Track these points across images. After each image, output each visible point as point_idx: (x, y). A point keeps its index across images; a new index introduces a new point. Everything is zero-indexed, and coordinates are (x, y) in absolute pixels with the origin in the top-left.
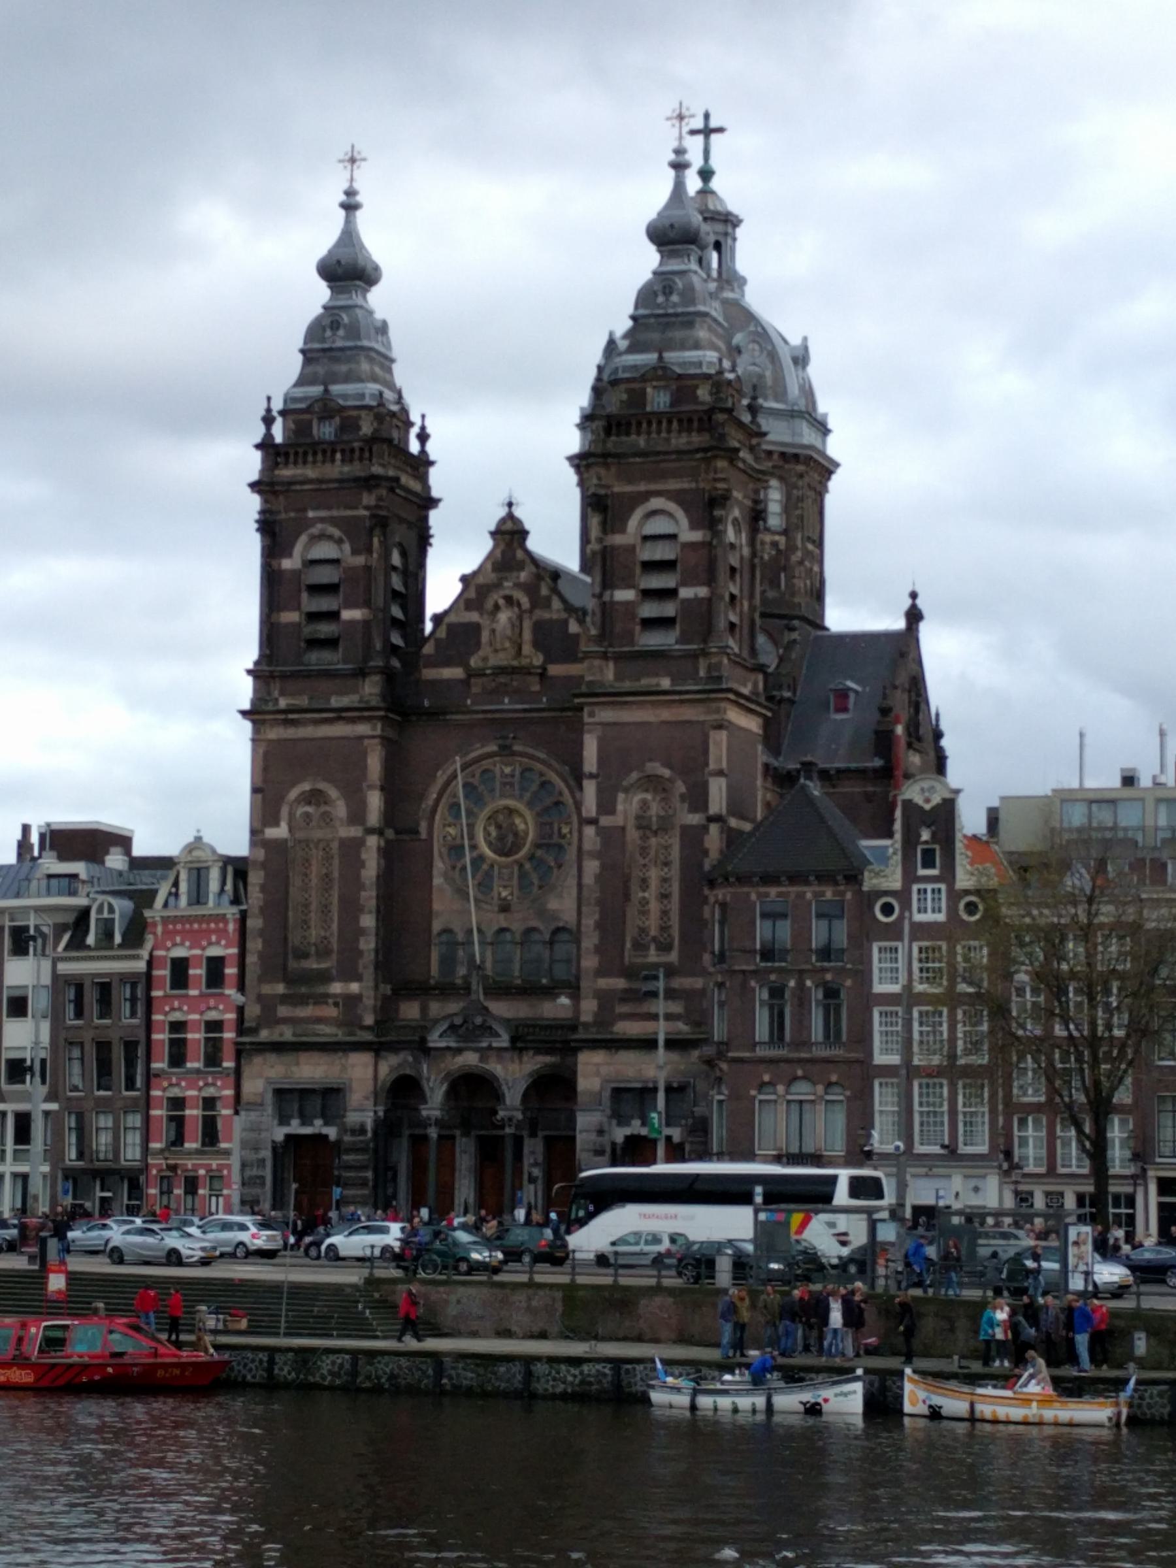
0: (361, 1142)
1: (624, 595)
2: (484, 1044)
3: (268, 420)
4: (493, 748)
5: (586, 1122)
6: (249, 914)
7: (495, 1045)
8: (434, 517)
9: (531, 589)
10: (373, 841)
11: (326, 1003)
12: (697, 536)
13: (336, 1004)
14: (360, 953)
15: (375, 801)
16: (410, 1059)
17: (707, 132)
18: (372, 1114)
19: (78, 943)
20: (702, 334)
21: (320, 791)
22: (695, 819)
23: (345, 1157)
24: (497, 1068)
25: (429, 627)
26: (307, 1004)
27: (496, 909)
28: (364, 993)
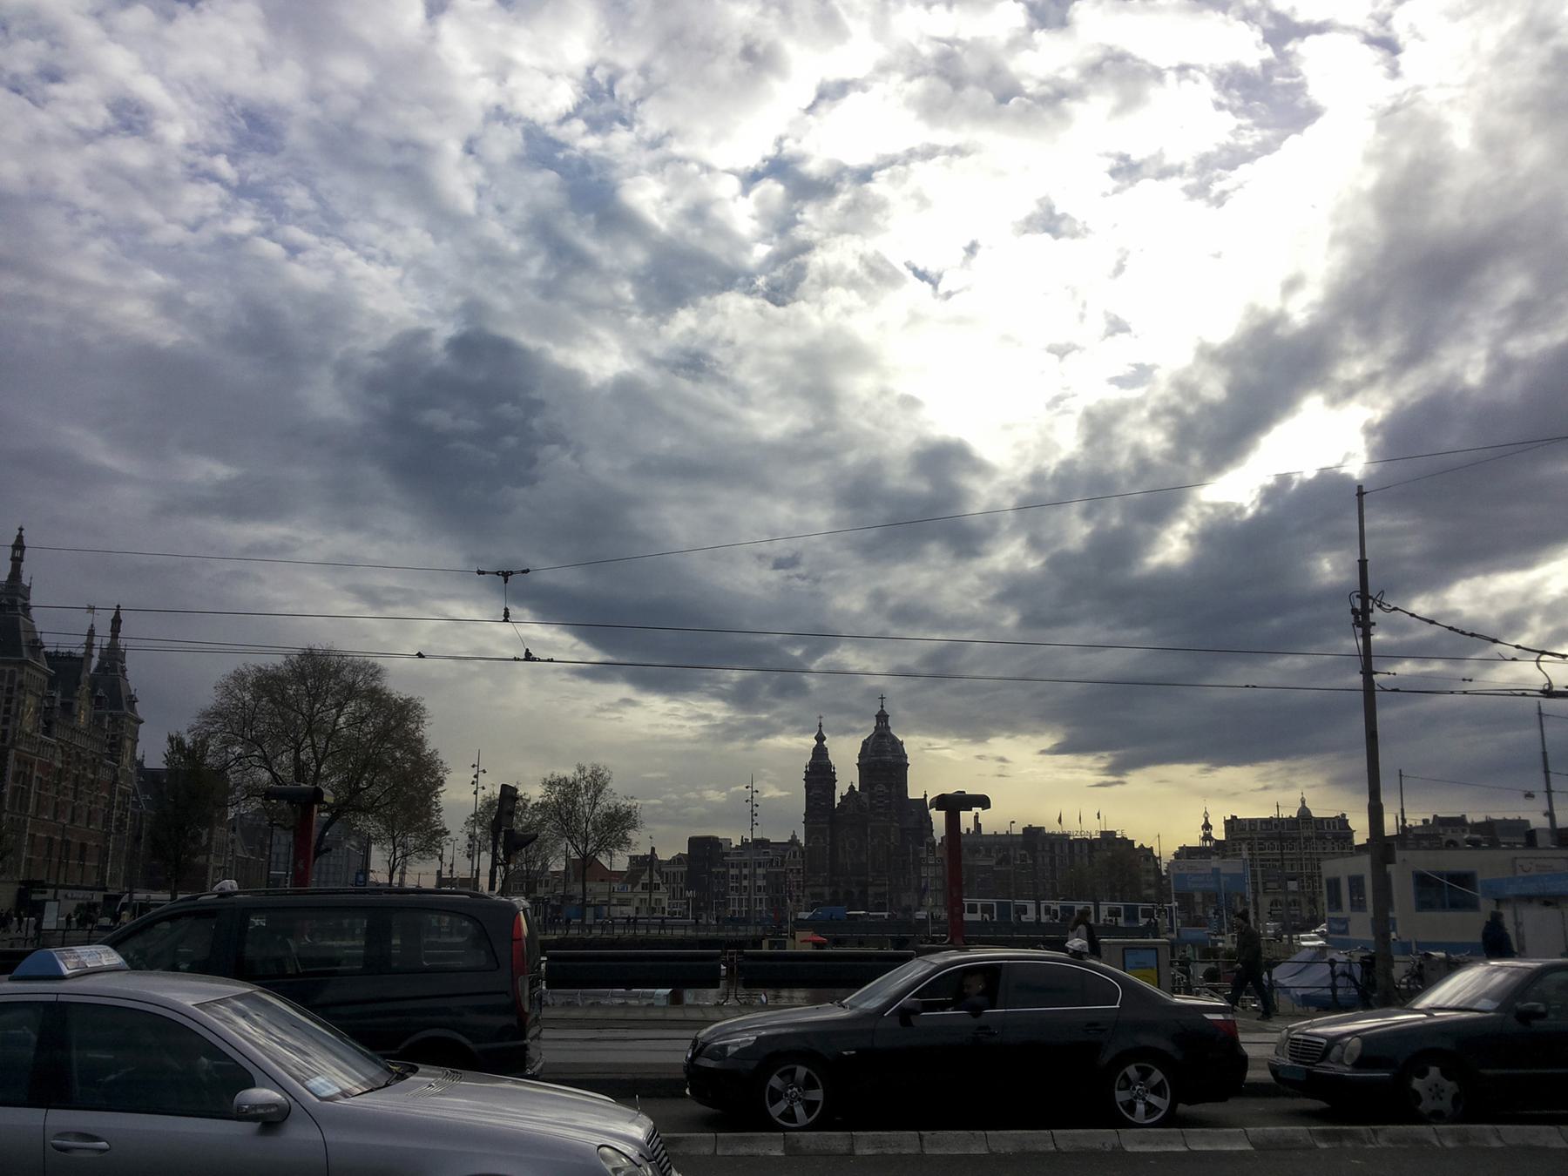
1: (874, 802)
3: (806, 767)
5: (870, 899)
8: (836, 784)
9: (856, 799)
12: (887, 791)
15: (828, 839)
17: (882, 698)
19: (771, 865)
20: (887, 754)
22: (888, 843)
24: (853, 890)
25: (836, 806)
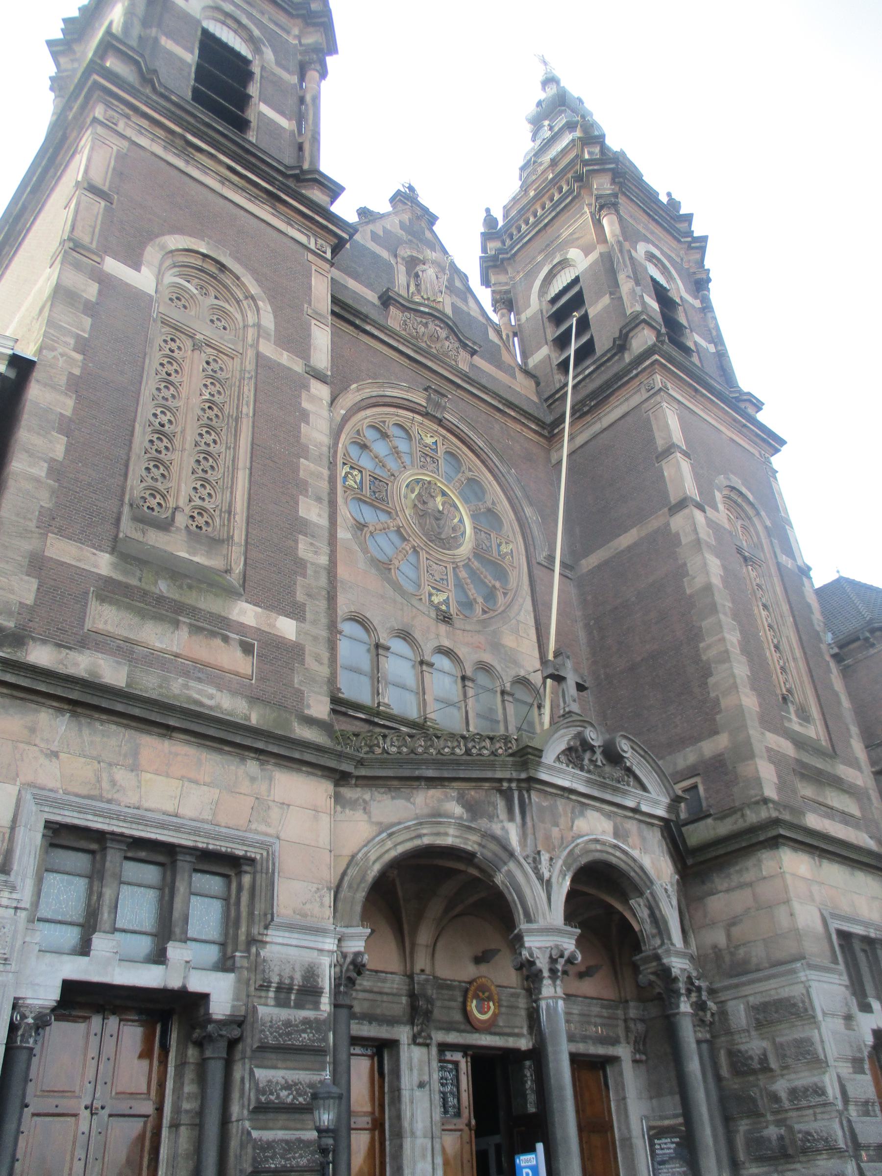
0: (306, 1022)
2: (631, 804)
4: (419, 398)
6: (37, 374)
7: (644, 808)
10: (321, 391)
11: (226, 639)
13: (247, 649)
14: (300, 565)
16: (458, 810)
18: (330, 944)
21: (222, 267)
23: (262, 1075)
26: (176, 624)
27: (433, 614)
28: (309, 648)
